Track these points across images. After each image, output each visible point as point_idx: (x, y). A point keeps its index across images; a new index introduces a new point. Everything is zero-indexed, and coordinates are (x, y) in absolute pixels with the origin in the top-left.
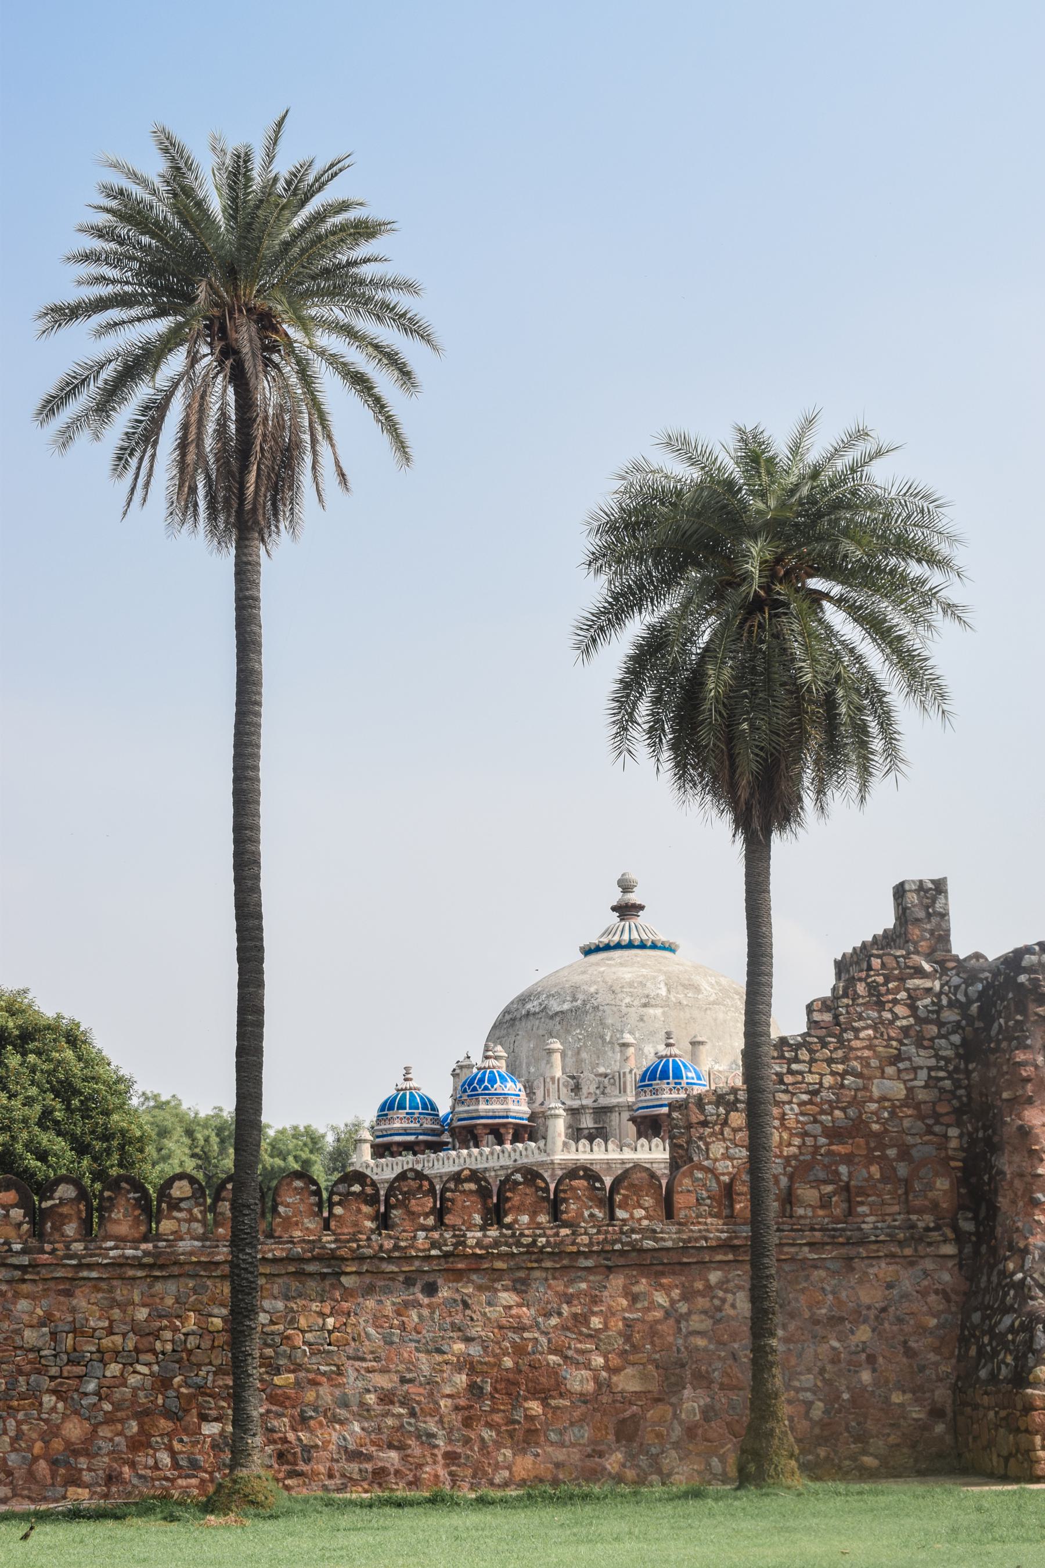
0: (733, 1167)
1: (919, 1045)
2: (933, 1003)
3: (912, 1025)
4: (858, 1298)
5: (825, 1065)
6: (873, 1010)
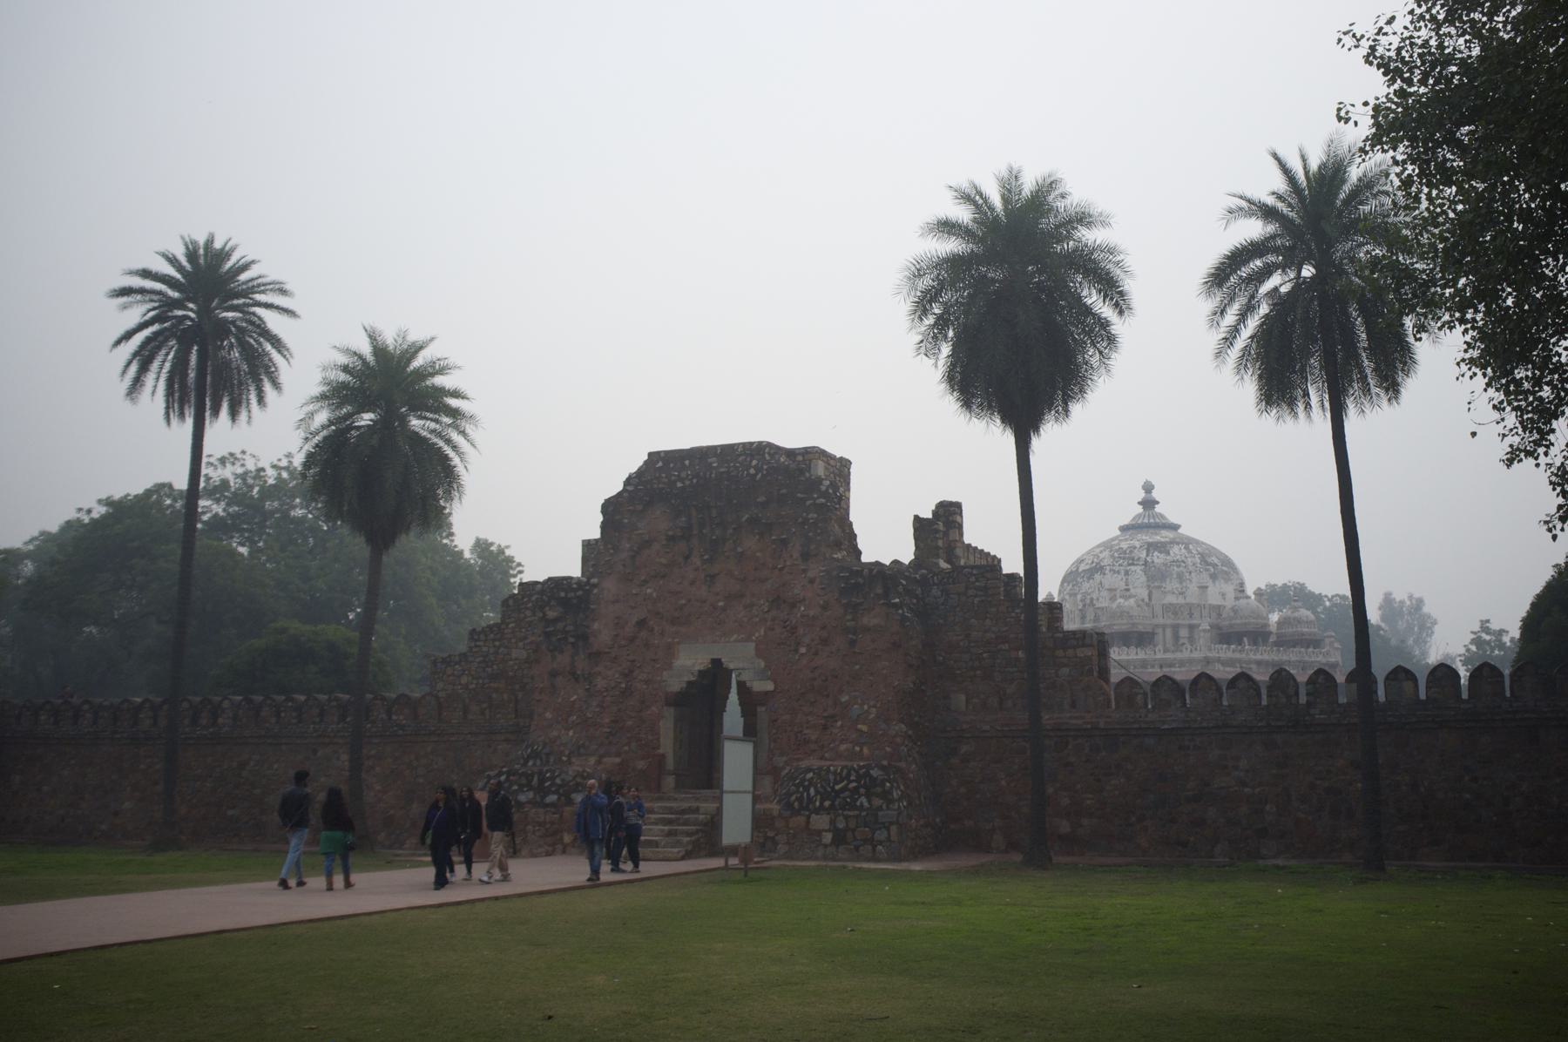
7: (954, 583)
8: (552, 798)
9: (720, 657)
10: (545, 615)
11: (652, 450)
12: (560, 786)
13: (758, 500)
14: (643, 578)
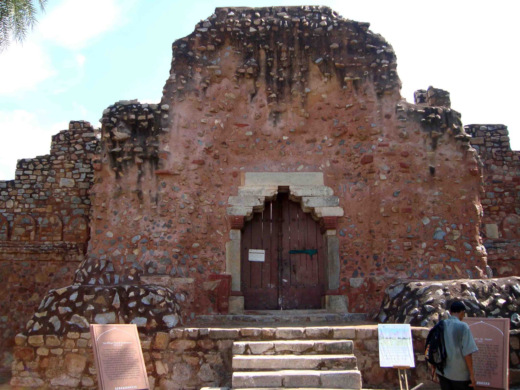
1: (84, 163)
3: (82, 154)
5: (40, 171)
9: (288, 185)
10: (112, 135)
11: (218, 7)
12: (149, 307)
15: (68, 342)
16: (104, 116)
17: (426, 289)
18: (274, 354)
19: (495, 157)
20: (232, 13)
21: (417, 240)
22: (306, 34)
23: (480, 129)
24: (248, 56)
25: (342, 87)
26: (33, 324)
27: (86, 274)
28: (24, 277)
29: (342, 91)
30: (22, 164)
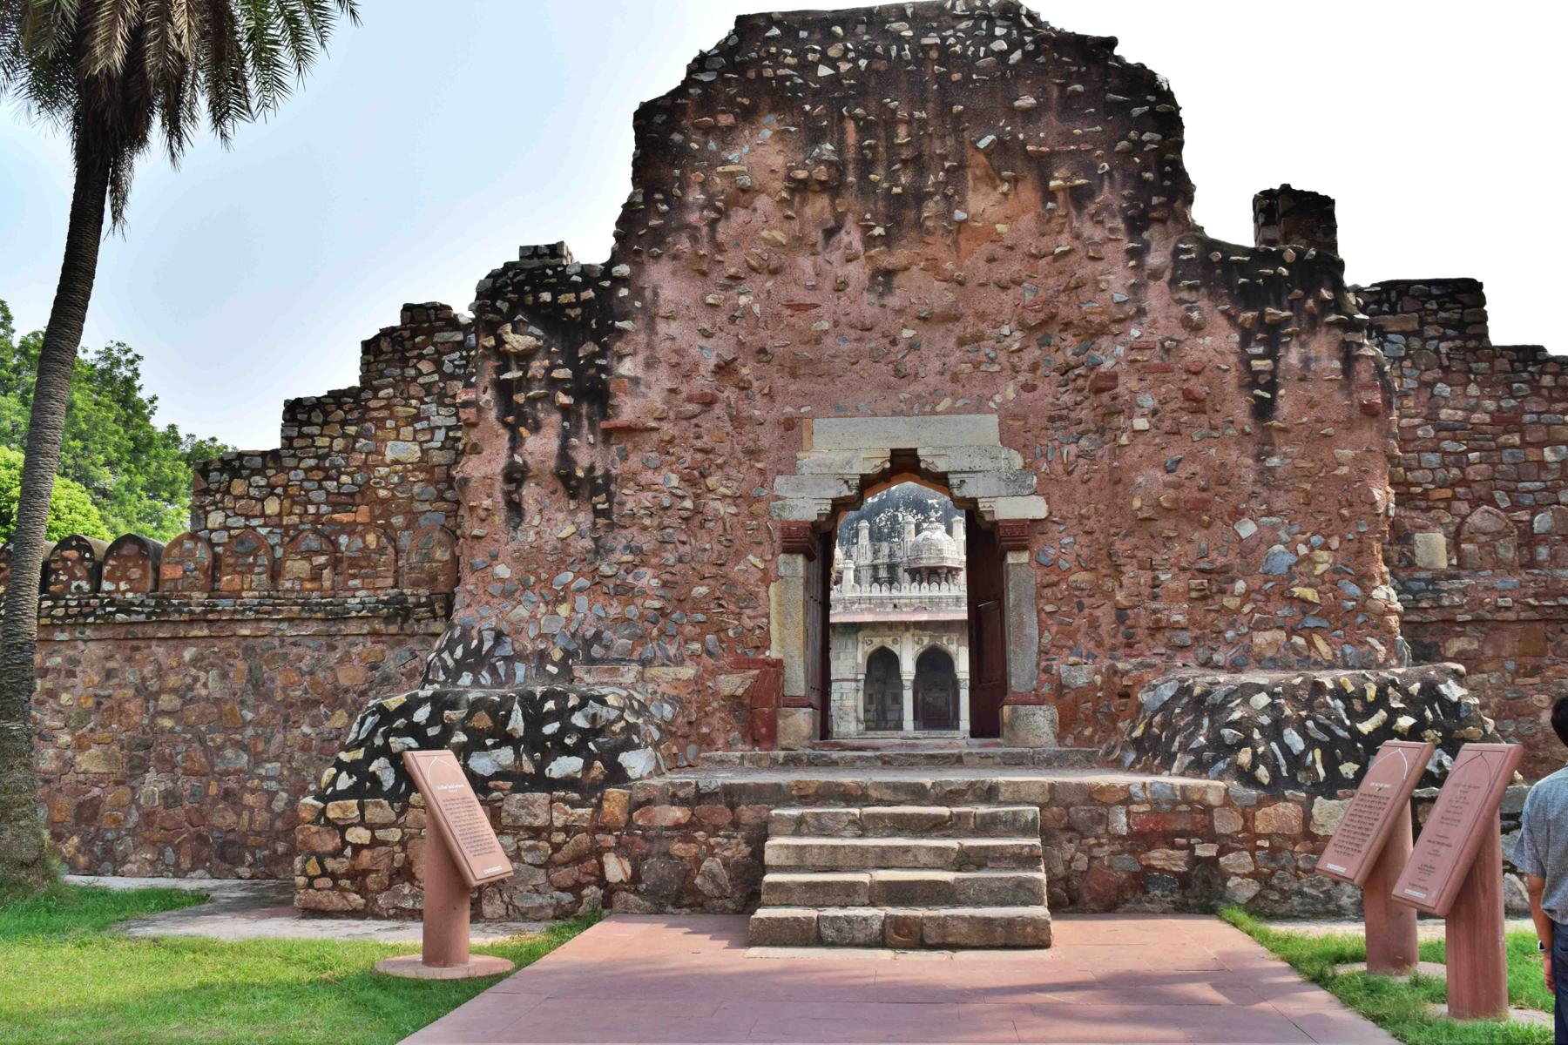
0: (230, 537)
1: (441, 404)
2: (462, 358)
4: (337, 680)
6: (396, 367)
7: (1393, 311)
8: (565, 766)
10: (501, 341)
12: (586, 735)
13: (1017, 103)
14: (732, 271)
15: (411, 815)
16: (480, 295)
17: (1229, 696)
18: (860, 836)
19: (1446, 363)
20: (775, 31)
21: (1222, 576)
22: (956, 77)
23: (1411, 293)
24: (815, 136)
25: (1044, 204)
26: (335, 778)
27: (450, 663)
28: (312, 673)
29: (1043, 215)
30: (294, 410)
